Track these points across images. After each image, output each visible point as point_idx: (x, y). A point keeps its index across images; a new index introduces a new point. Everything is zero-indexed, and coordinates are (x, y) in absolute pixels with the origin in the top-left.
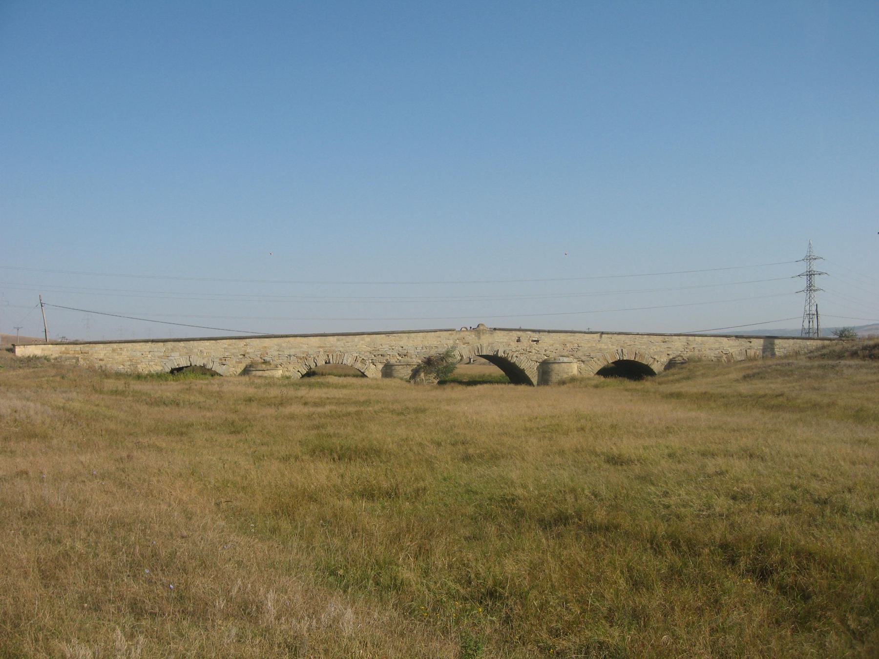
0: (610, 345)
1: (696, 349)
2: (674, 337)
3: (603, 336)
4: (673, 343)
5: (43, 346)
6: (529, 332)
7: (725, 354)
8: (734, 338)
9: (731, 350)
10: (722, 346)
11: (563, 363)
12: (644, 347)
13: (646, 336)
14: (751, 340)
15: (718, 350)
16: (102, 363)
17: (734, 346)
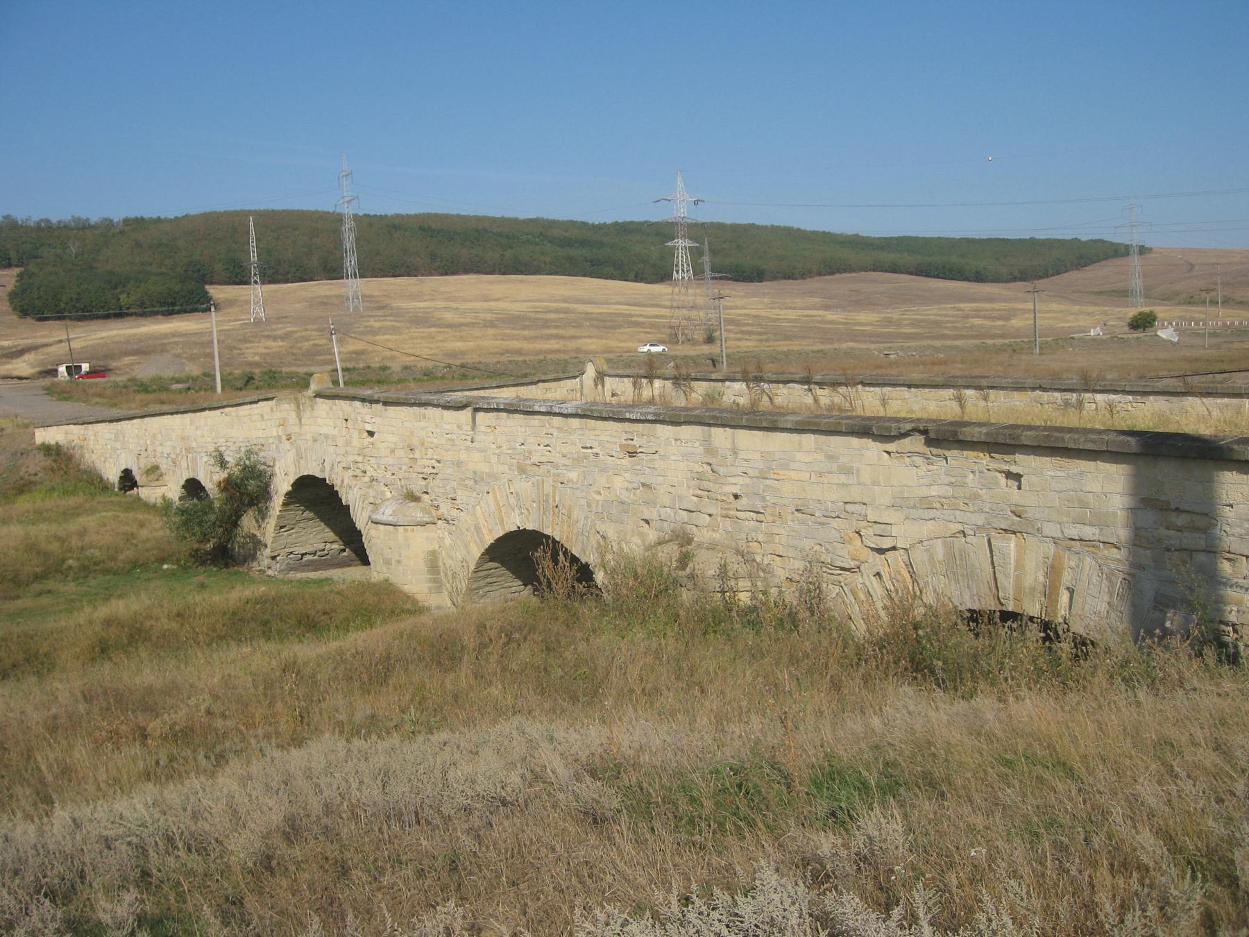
0: (494, 460)
1: (743, 502)
2: (659, 427)
3: (480, 415)
4: (659, 464)
5: (72, 426)
6: (357, 404)
7: (881, 551)
8: (916, 443)
9: (904, 532)
10: (855, 493)
11: (381, 524)
12: (573, 475)
13: (575, 422)
14: (1023, 463)
15: (835, 523)
16: (94, 457)
17: (926, 503)
